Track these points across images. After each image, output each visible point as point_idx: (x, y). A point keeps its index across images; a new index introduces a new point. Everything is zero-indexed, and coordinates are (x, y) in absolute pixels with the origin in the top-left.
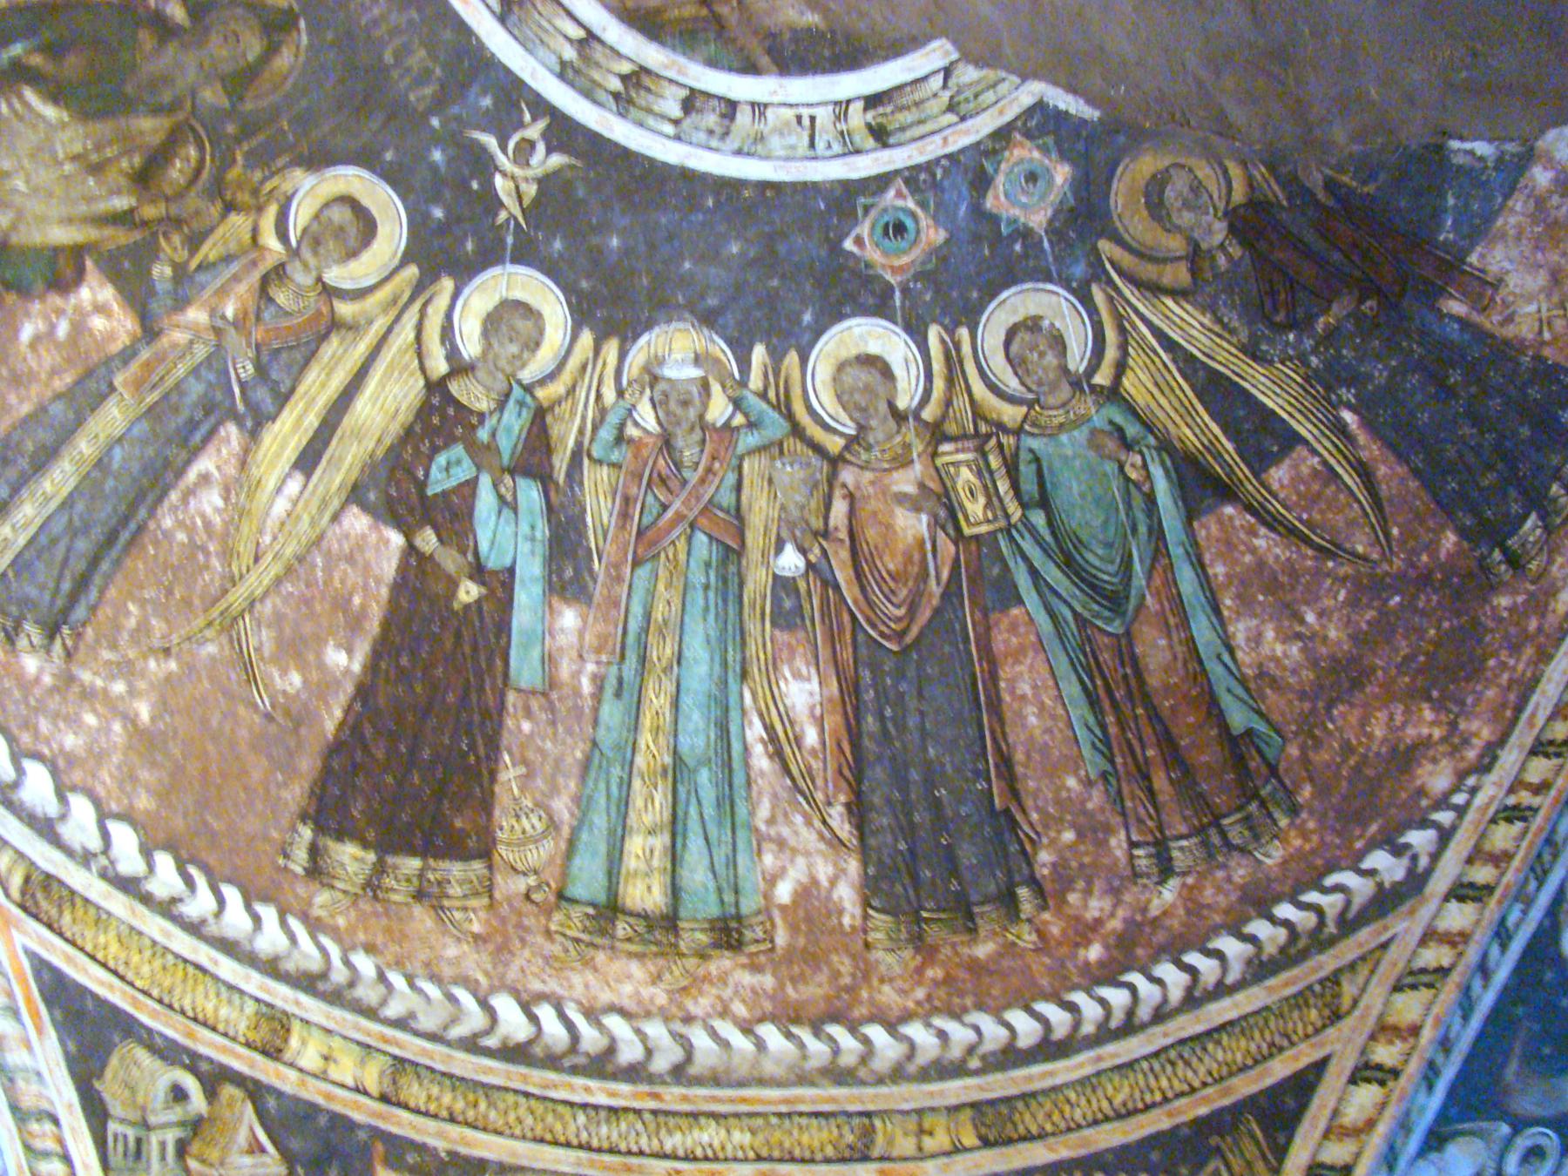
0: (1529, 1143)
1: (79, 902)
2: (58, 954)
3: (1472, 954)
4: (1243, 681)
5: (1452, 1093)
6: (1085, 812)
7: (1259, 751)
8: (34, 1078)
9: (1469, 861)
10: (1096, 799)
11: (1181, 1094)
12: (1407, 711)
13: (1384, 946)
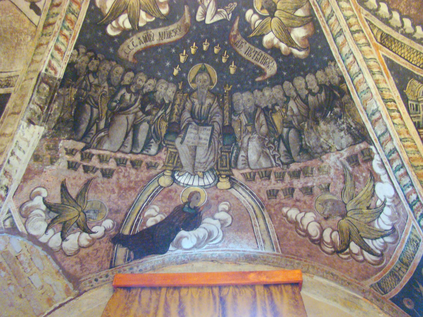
1: (396, 41)
2: (391, 56)
8: (387, 90)
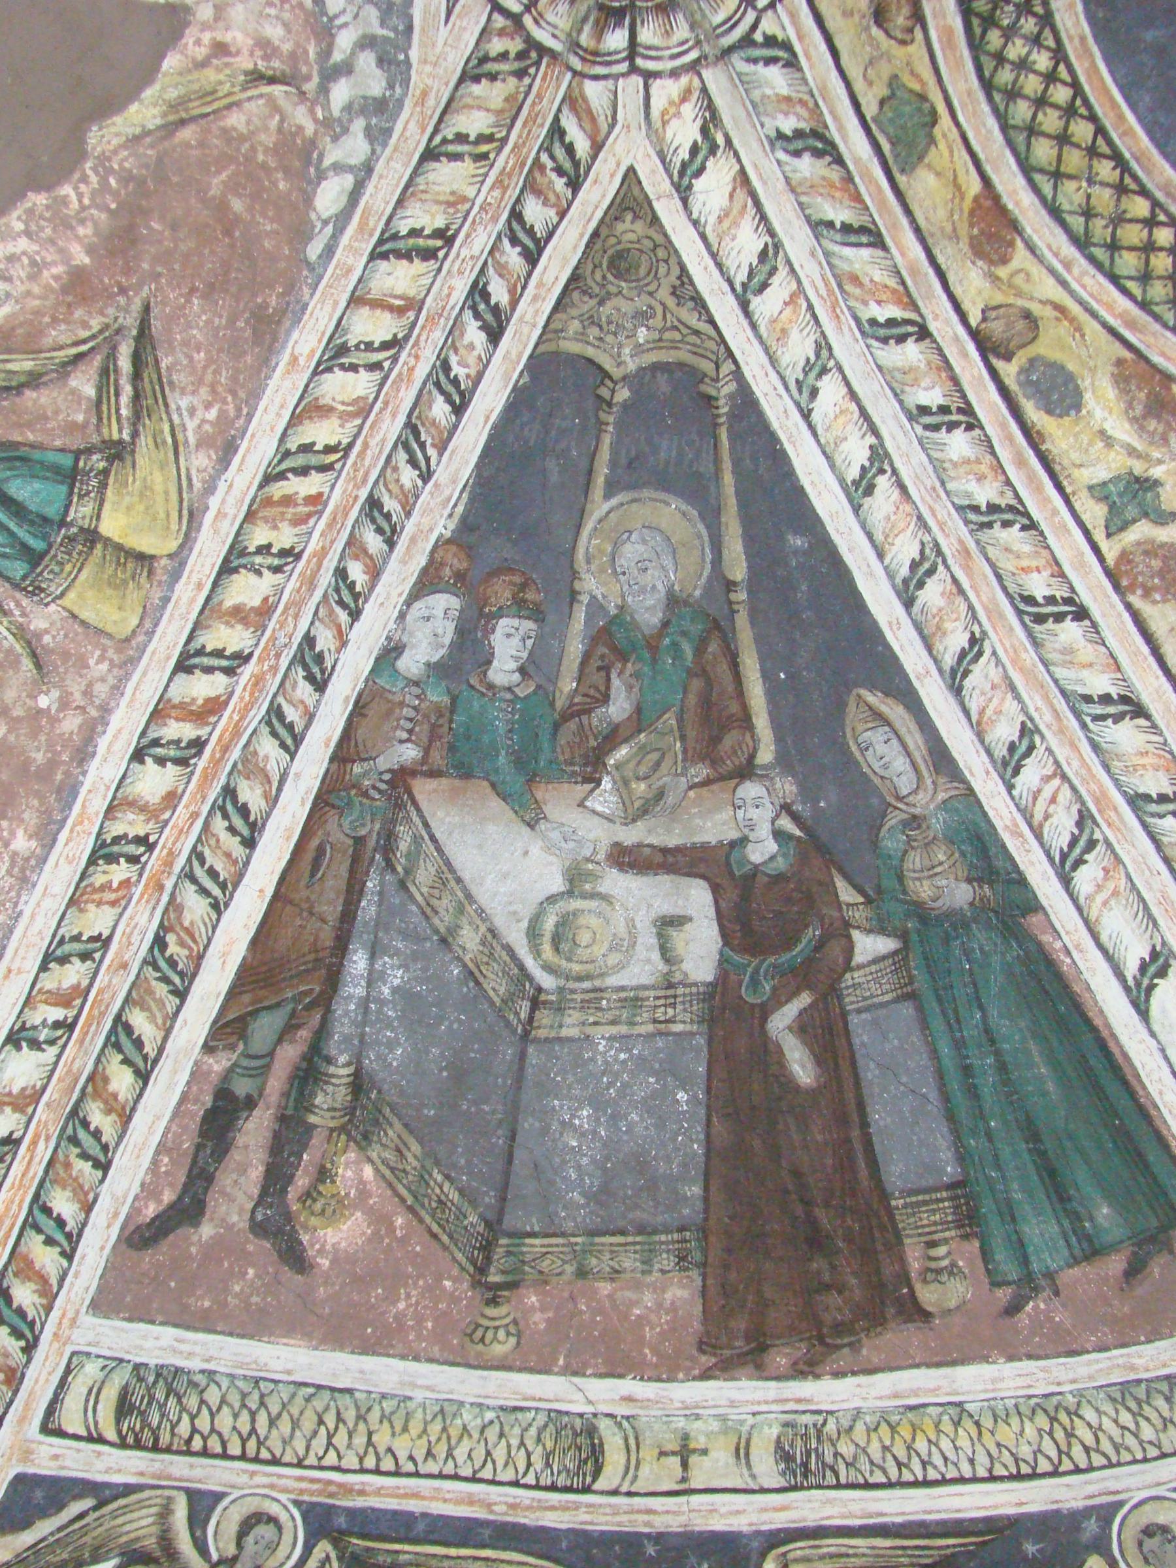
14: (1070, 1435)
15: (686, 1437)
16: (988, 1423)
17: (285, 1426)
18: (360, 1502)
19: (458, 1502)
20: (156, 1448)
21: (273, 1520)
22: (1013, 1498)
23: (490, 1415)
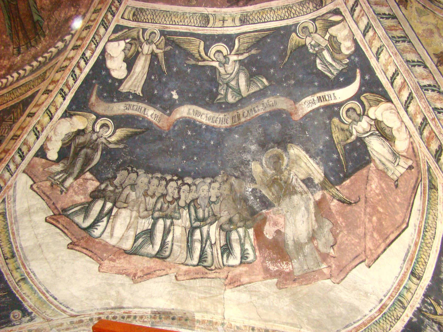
0: (103, 122)
3: (74, 62)
4: (37, 10)
5: (72, 101)
6: (6, 43)
7: (39, 24)
9: (77, 40)
10: (8, 39)
11: (11, 100)
12: (69, 10)
13: (57, 63)
14: (291, 12)
15: (224, 18)
16: (276, 11)
17: (158, 17)
18: (169, 30)
19: (185, 29)
20: (138, 22)
21: (155, 33)
22: (280, 24)
23: (191, 14)
